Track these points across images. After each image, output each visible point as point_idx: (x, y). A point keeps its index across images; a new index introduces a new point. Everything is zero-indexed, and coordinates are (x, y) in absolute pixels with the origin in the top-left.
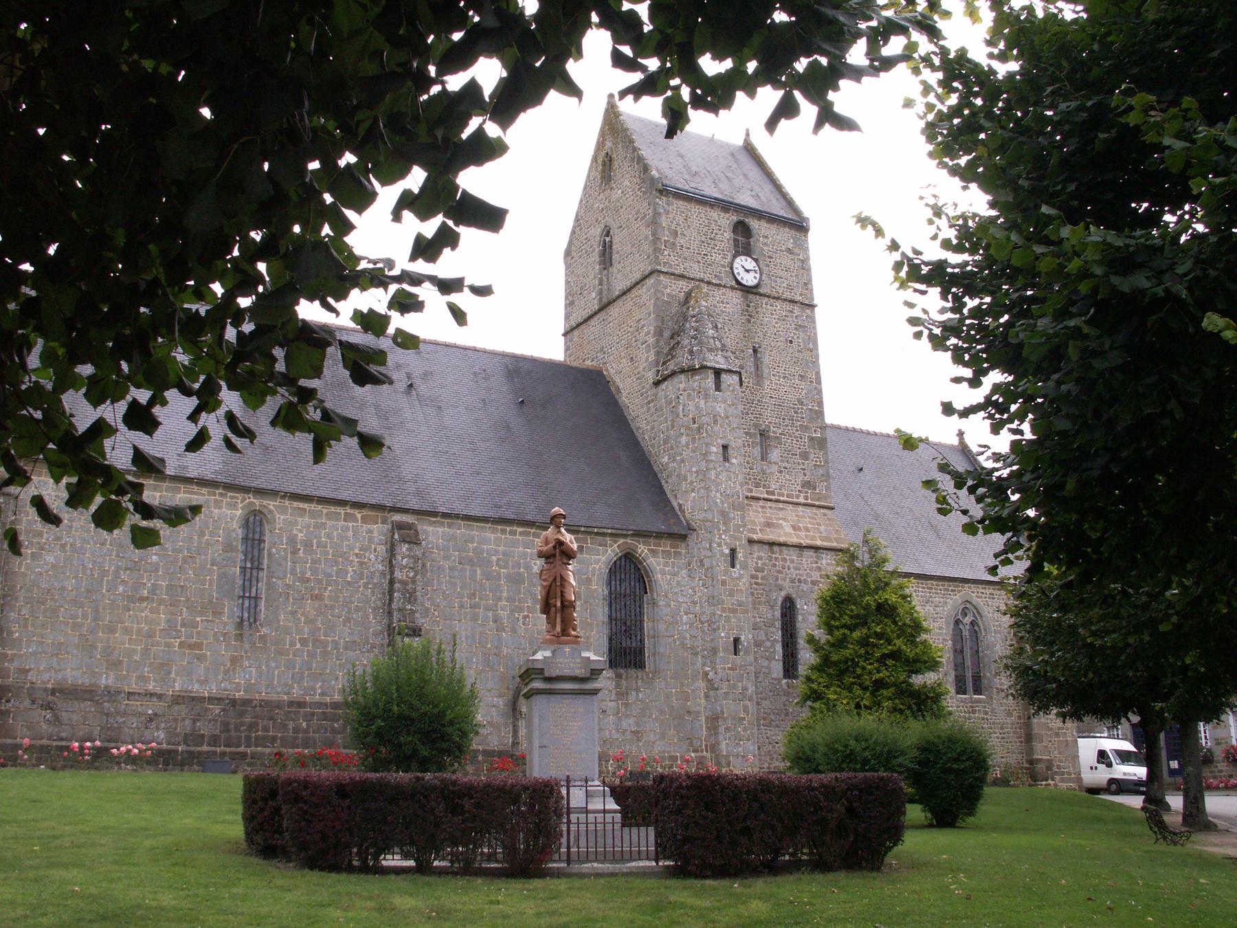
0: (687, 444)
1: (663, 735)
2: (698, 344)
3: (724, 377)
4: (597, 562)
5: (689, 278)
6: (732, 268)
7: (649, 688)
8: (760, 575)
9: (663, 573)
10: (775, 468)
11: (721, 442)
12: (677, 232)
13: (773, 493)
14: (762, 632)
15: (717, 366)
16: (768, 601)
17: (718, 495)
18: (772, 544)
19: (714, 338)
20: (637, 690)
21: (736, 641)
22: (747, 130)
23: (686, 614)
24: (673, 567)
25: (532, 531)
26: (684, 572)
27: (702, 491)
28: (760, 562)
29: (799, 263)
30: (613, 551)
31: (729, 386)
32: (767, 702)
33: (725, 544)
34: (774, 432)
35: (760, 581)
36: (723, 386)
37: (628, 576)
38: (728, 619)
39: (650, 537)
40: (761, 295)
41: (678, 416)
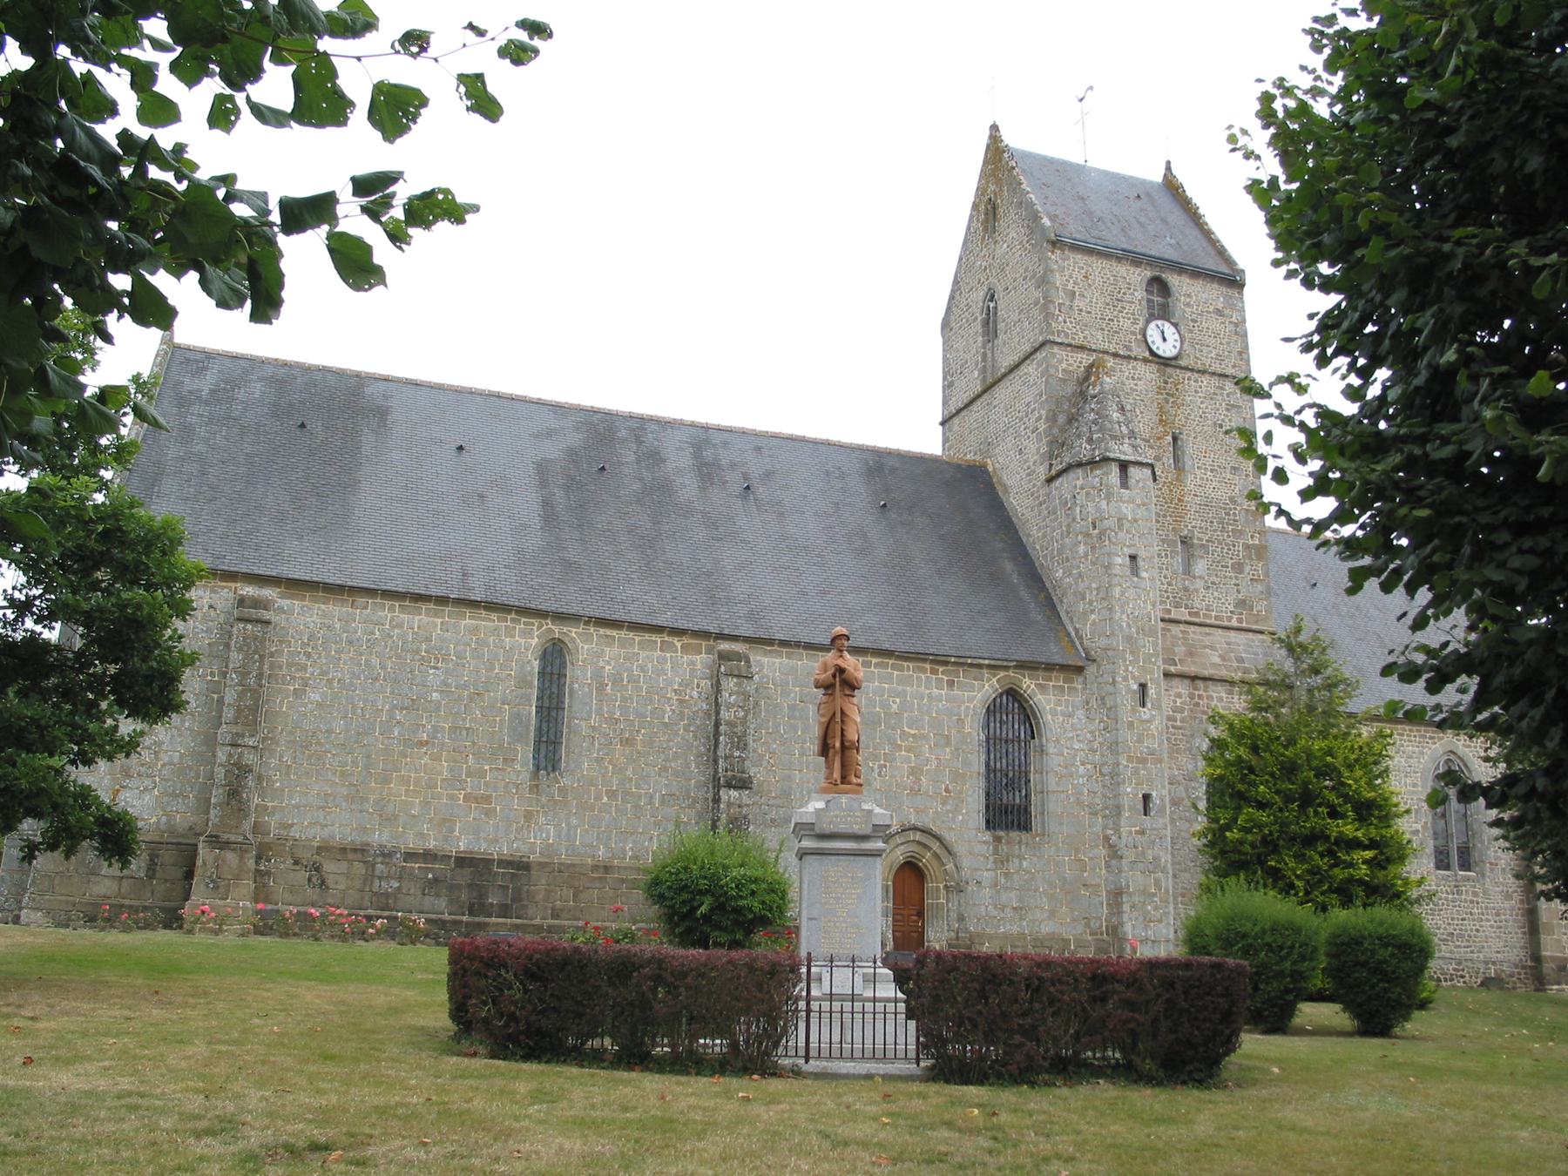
0: (1086, 556)
1: (1052, 913)
2: (1099, 431)
3: (1133, 472)
4: (971, 699)
5: (1090, 350)
6: (1144, 336)
7: (1034, 855)
8: (1179, 716)
9: (1054, 713)
10: (1199, 584)
11: (1127, 551)
12: (1074, 293)
13: (1197, 614)
14: (1181, 788)
15: (1123, 457)
16: (1190, 749)
17: (1124, 617)
18: (1194, 678)
19: (1119, 423)
20: (1021, 858)
21: (1146, 798)
22: (1168, 163)
23: (1083, 764)
24: (1067, 707)
25: (891, 662)
26: (1080, 713)
27: (1104, 612)
28: (1178, 700)
29: (1232, 327)
30: (992, 686)
31: (1138, 481)
32: (1187, 875)
33: (1134, 677)
34: (1199, 539)
35: (1178, 723)
36: (1132, 482)
37: (1010, 717)
38: (1136, 772)
39: (1037, 669)
40: (1186, 368)
41: (1074, 520)
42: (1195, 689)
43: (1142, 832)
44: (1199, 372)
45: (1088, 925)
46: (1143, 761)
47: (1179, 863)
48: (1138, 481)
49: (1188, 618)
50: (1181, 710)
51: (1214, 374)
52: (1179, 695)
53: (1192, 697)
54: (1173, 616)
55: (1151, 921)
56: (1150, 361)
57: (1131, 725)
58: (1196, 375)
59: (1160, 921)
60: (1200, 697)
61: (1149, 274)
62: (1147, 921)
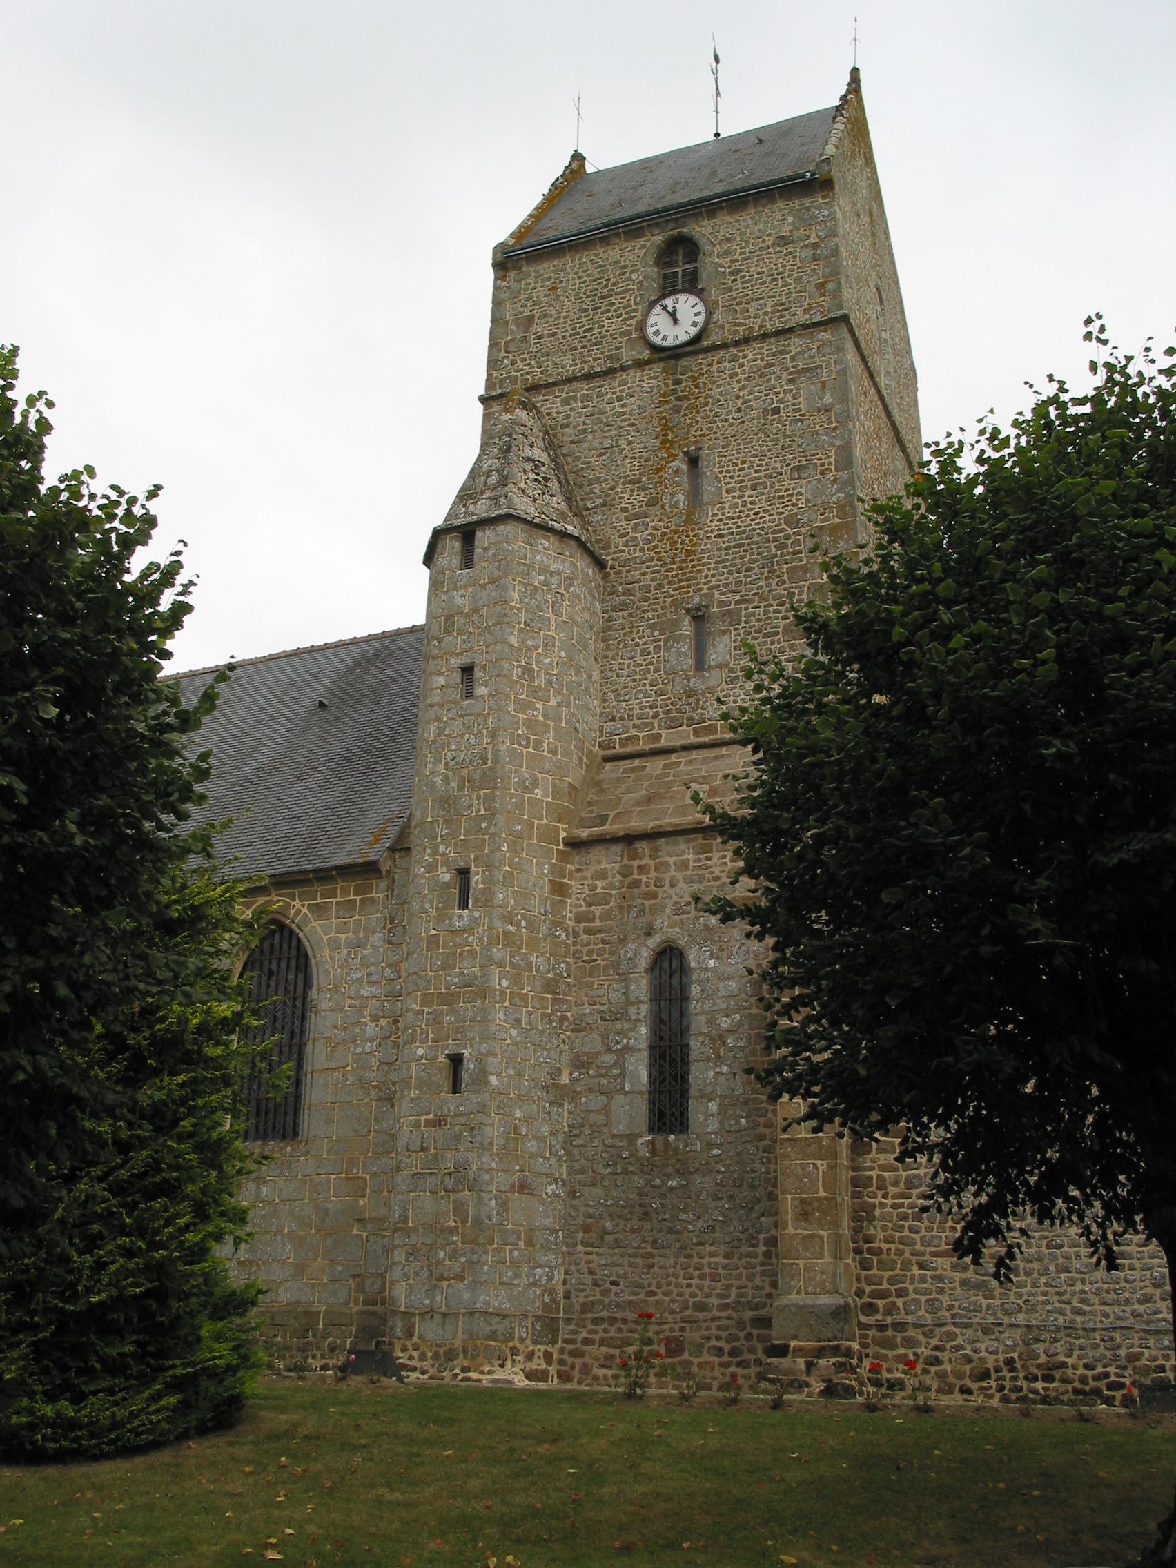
1: (300, 1269)
5: (547, 386)
7: (282, 1175)
8: (597, 911)
9: (334, 946)
11: (455, 662)
13: (711, 729)
14: (595, 1035)
16: (616, 965)
17: (440, 768)
18: (629, 839)
20: (260, 1181)
21: (456, 1061)
22: (855, 72)
23: (375, 1018)
24: (356, 932)
26: (377, 938)
28: (599, 884)
31: (486, 549)
32: (597, 1191)
33: (446, 863)
34: (721, 604)
35: (598, 924)
37: (284, 964)
38: (437, 1020)
39: (307, 882)
40: (714, 348)
42: (634, 857)
43: (438, 1122)
44: (737, 344)
45: (361, 1288)
46: (449, 999)
47: (582, 1172)
48: (486, 549)
49: (693, 740)
50: (605, 900)
51: (765, 336)
52: (602, 875)
53: (625, 873)
54: (663, 743)
55: (441, 1278)
56: (648, 362)
57: (433, 942)
58: (734, 351)
59: (461, 1278)
60: (641, 869)
61: (658, 239)
62: (437, 1278)
